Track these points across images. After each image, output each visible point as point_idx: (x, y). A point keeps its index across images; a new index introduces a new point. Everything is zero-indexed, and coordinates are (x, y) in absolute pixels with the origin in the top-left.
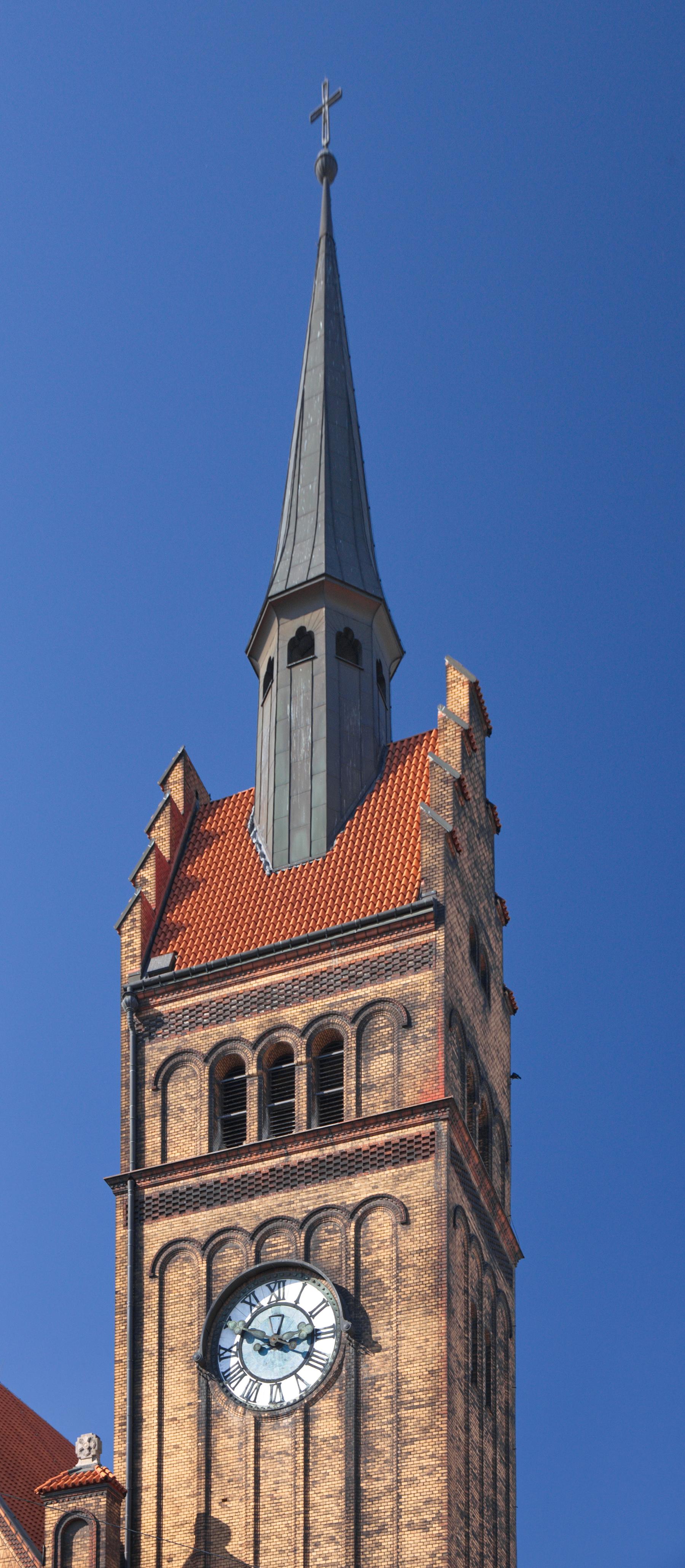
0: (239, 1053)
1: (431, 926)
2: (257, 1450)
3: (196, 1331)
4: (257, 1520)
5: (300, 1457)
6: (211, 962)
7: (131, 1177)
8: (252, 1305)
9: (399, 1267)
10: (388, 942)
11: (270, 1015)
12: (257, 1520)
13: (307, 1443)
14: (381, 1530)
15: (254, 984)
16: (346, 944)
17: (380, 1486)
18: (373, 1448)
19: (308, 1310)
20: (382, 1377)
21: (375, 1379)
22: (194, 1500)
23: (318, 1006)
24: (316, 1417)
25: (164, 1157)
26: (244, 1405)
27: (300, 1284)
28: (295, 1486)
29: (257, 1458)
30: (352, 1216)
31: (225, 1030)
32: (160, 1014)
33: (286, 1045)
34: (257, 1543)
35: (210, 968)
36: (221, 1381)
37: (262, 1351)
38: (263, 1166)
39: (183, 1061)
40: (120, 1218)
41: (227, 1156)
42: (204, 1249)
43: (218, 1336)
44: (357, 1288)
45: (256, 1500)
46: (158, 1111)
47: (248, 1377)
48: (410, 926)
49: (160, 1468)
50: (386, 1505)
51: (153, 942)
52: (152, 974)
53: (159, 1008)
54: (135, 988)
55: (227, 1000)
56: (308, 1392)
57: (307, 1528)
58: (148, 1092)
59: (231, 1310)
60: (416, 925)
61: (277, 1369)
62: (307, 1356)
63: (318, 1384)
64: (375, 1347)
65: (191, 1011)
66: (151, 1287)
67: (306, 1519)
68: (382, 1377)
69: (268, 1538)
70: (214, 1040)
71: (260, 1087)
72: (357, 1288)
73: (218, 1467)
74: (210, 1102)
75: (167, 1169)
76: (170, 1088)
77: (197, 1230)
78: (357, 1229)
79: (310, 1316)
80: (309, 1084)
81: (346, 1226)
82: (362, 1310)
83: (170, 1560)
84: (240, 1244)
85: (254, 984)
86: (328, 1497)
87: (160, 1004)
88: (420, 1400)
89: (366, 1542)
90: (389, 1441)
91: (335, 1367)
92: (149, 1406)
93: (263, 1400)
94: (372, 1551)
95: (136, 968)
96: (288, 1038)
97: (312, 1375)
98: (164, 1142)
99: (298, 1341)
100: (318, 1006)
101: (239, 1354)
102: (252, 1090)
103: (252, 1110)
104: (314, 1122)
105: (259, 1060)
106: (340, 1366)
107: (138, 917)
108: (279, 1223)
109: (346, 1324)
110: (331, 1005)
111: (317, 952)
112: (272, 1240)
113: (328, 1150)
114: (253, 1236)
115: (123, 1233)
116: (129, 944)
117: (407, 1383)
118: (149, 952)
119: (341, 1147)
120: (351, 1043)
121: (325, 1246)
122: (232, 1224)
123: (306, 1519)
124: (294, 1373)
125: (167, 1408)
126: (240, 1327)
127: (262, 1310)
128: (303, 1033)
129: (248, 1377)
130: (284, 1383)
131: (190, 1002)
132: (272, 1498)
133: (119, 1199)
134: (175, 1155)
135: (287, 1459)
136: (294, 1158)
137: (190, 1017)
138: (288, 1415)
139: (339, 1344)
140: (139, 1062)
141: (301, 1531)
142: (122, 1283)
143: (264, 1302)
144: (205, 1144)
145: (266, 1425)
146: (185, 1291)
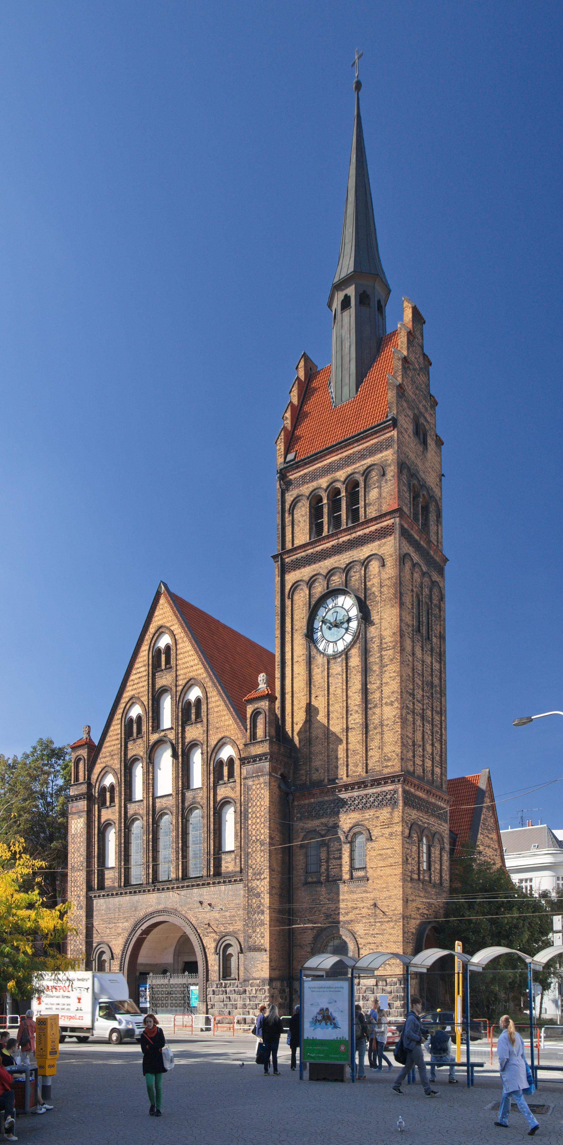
1: (392, 429)
2: (328, 673)
3: (305, 621)
4: (328, 705)
5: (344, 676)
6: (309, 455)
7: (280, 554)
8: (326, 608)
9: (381, 586)
10: (376, 438)
11: (332, 476)
12: (328, 705)
13: (347, 669)
14: (375, 707)
15: (325, 462)
16: (359, 441)
17: (374, 686)
18: (372, 670)
19: (347, 609)
20: (375, 637)
21: (372, 638)
22: (305, 697)
23: (349, 470)
24: (350, 657)
25: (293, 544)
26: (323, 653)
27: (343, 597)
28: (343, 689)
29: (328, 677)
30: (363, 565)
31: (314, 484)
32: (291, 480)
33: (338, 488)
34: (328, 715)
35: (309, 458)
36: (314, 643)
37: (330, 628)
38: (329, 545)
40: (277, 573)
41: (316, 542)
42: (307, 584)
43: (313, 623)
44: (365, 597)
45: (328, 696)
46: (291, 523)
47: (325, 641)
48: (384, 430)
49: (292, 683)
50: (377, 695)
51: (289, 446)
52: (287, 463)
53: (290, 477)
54: (281, 470)
56: (347, 646)
57: (347, 707)
58: (287, 515)
59: (318, 611)
60: (386, 429)
61: (335, 636)
62: (347, 629)
63: (351, 642)
64: (372, 623)
66: (288, 603)
67: (347, 703)
68: (375, 637)
69: (333, 712)
70: (311, 489)
71: (328, 508)
72: (365, 597)
73: (314, 682)
74: (310, 517)
75: (294, 550)
76: (295, 512)
78: (365, 571)
79: (347, 611)
80: (346, 505)
81: (361, 569)
82: (367, 607)
83: (297, 724)
84: (321, 581)
85: (325, 462)
86: (356, 692)
88: (390, 646)
89: (370, 712)
90: (378, 666)
91: (357, 634)
92: (288, 656)
93: (330, 651)
94: (372, 716)
95: (281, 460)
96: (338, 485)
97: (348, 638)
98: (293, 537)
99: (342, 623)
100: (349, 470)
101: (321, 630)
102: (325, 510)
103: (325, 519)
104: (350, 522)
105: (328, 496)
106: (359, 633)
107: (282, 437)
108: (335, 570)
109: (360, 614)
110: (355, 469)
111: (349, 446)
112: (333, 578)
113: (354, 535)
114: (326, 577)
115: (278, 579)
116: (279, 450)
117: (385, 639)
118: (287, 452)
119: (358, 533)
120: (362, 485)
121: (353, 579)
122: (318, 572)
123: (347, 703)
124: (342, 638)
125: (295, 657)
126: (321, 619)
127: (330, 610)
128: (344, 483)
129: (325, 641)
130: (338, 643)
131: (302, 473)
132: (334, 695)
133: (276, 564)
134: (298, 542)
135: (340, 677)
136: (341, 540)
138: (340, 657)
139: (358, 623)
140: (283, 502)
141: (345, 709)
142: (278, 603)
143: (330, 607)
144: (308, 538)
145: (332, 662)
146: (301, 603)
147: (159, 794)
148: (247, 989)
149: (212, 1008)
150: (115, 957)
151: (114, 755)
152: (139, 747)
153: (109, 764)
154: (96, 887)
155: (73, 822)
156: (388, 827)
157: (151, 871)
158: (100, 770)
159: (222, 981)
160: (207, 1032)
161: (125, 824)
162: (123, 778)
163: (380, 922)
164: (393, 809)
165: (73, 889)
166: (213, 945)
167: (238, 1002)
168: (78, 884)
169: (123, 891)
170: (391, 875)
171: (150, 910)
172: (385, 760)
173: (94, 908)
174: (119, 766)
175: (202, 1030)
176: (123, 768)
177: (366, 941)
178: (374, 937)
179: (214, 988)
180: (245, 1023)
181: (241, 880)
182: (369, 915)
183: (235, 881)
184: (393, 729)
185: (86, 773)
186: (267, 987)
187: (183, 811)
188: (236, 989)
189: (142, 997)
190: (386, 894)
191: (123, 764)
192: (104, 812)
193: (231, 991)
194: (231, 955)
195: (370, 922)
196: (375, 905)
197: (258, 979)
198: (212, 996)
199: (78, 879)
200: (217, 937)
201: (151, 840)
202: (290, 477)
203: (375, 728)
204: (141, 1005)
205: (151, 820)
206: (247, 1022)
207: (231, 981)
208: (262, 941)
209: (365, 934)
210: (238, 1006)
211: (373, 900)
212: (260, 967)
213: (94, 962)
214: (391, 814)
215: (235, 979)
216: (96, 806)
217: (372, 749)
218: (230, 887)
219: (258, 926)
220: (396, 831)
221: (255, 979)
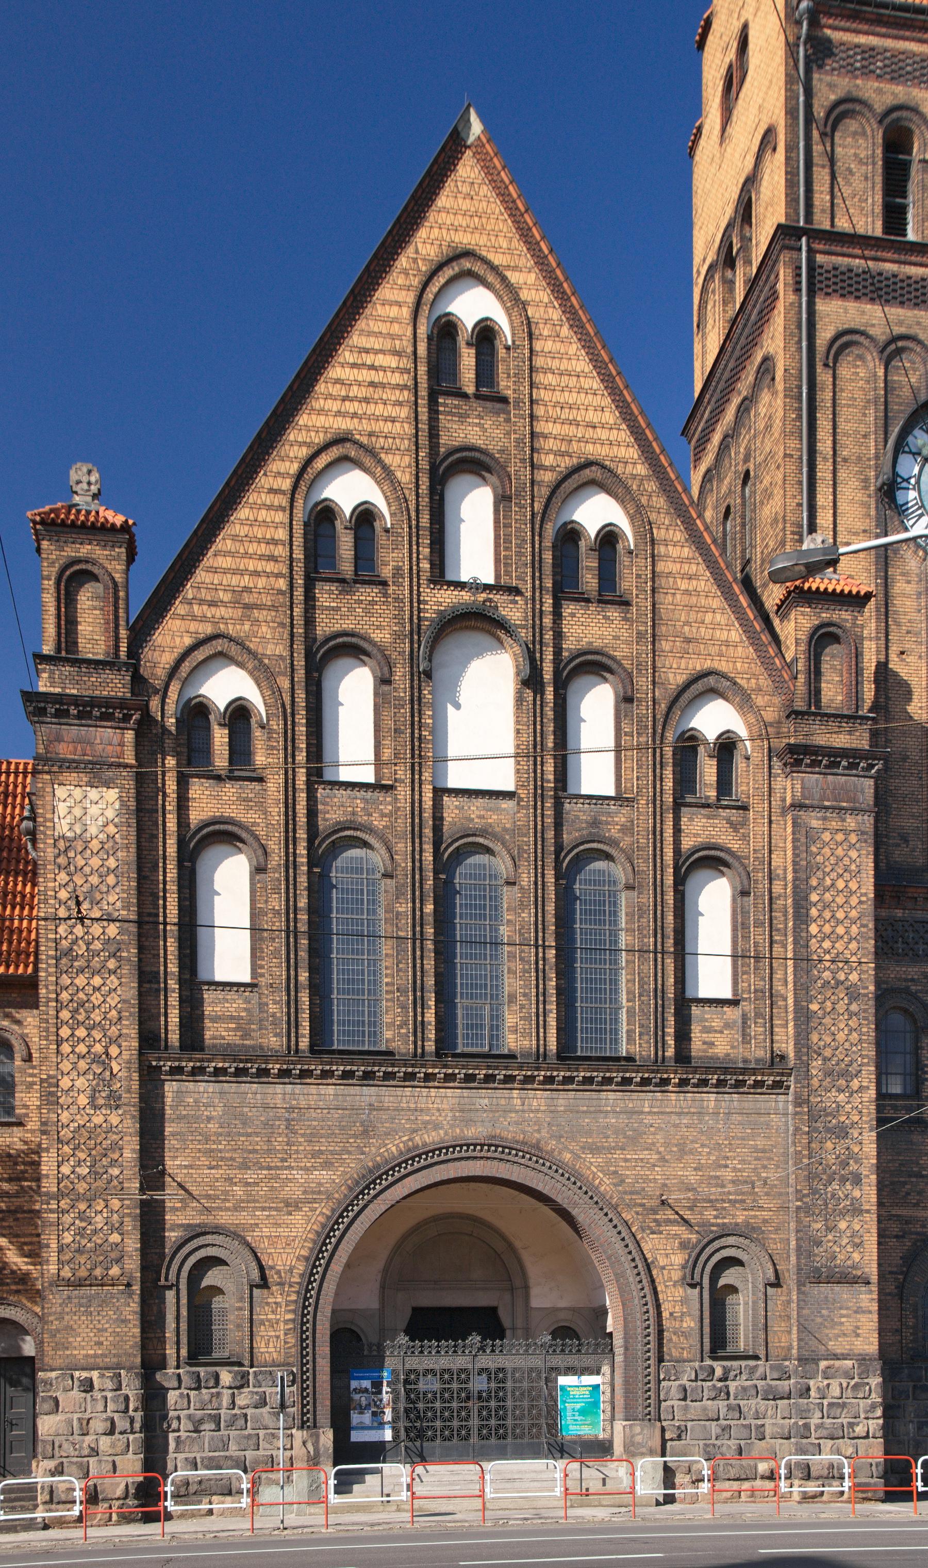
0: (913, 127)
39: (853, 111)
53: (828, 32)
55: (901, 57)
65: (863, 52)
70: (889, 101)
87: (830, 27)
131: (862, 39)
137: (863, 59)
147: (451, 784)
148: (812, 1383)
149: (679, 1438)
150: (272, 1277)
152: (367, 612)
153: (231, 630)
154: (174, 1037)
155: (61, 792)
157: (430, 1016)
158: (188, 641)
159: (708, 1362)
160: (669, 1507)
161: (310, 848)
162: (301, 695)
165: (65, 1032)
166: (678, 1259)
167: (768, 1422)
168: (96, 1017)
169: (318, 1069)
171: (431, 1138)
173: (168, 1111)
174: (281, 650)
175: (658, 1504)
176: (300, 662)
179: (684, 1381)
180: (808, 1477)
181: (777, 1085)
183: (758, 1084)
185: (123, 633)
186: (875, 1381)
187: (557, 853)
188: (760, 1384)
189: (362, 1410)
191: (299, 647)
192: (198, 789)
193: (744, 1389)
194: (732, 1289)
197: (845, 1357)
198: (676, 1403)
199: (96, 999)
200: (694, 1237)
201: (430, 919)
202: (828, 32)
204: (356, 1436)
205: (428, 857)
206: (813, 1474)
207: (743, 1363)
208: (856, 1256)
210: (768, 1431)
212: (848, 1324)
213: (170, 1295)
215: (757, 1358)
216: (171, 762)
218: (734, 1100)
219: (842, 1214)
221: (836, 1357)
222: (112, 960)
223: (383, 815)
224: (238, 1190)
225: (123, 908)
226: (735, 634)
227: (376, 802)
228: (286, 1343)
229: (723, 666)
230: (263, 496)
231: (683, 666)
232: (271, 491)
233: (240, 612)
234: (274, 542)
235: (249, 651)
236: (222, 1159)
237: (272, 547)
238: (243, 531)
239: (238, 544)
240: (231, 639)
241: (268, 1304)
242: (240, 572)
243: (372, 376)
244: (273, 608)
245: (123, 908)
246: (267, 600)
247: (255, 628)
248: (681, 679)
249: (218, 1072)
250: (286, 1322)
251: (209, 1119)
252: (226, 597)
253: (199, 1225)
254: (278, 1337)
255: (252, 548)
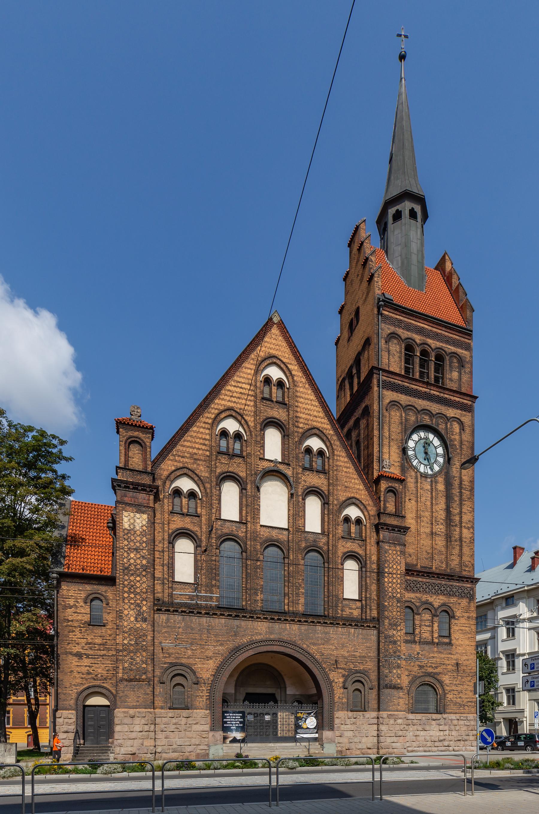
14: (456, 526)
77: (401, 401)
122: (413, 404)
151: (199, 460)
152: (238, 466)
153: (189, 466)
156: (467, 612)
163: (460, 676)
164: (470, 600)
170: (468, 645)
172: (464, 565)
174: (207, 475)
177: (451, 688)
178: (457, 686)
182: (453, 670)
184: (469, 546)
190: (465, 658)
195: (454, 676)
196: (457, 664)
203: (456, 541)
209: (450, 684)
211: (456, 660)
214: (469, 604)
217: (454, 555)
220: (472, 616)
222: (144, 572)
223: (242, 532)
224: (189, 652)
225: (148, 555)
226: (361, 487)
227: (240, 527)
228: (206, 703)
229: (358, 496)
230: (202, 424)
231: (344, 495)
232: (205, 423)
233: (193, 461)
234: (205, 439)
235: (196, 474)
236: (184, 641)
237: (205, 441)
238: (195, 434)
239: (192, 438)
240: (189, 469)
241: (200, 690)
242: (194, 448)
243: (241, 390)
244: (205, 461)
245: (148, 555)
246: (203, 458)
247: (198, 467)
248: (344, 499)
249: (182, 612)
250: (207, 696)
251: (179, 628)
252: (188, 455)
253: (174, 663)
254: (203, 701)
255: (197, 440)
